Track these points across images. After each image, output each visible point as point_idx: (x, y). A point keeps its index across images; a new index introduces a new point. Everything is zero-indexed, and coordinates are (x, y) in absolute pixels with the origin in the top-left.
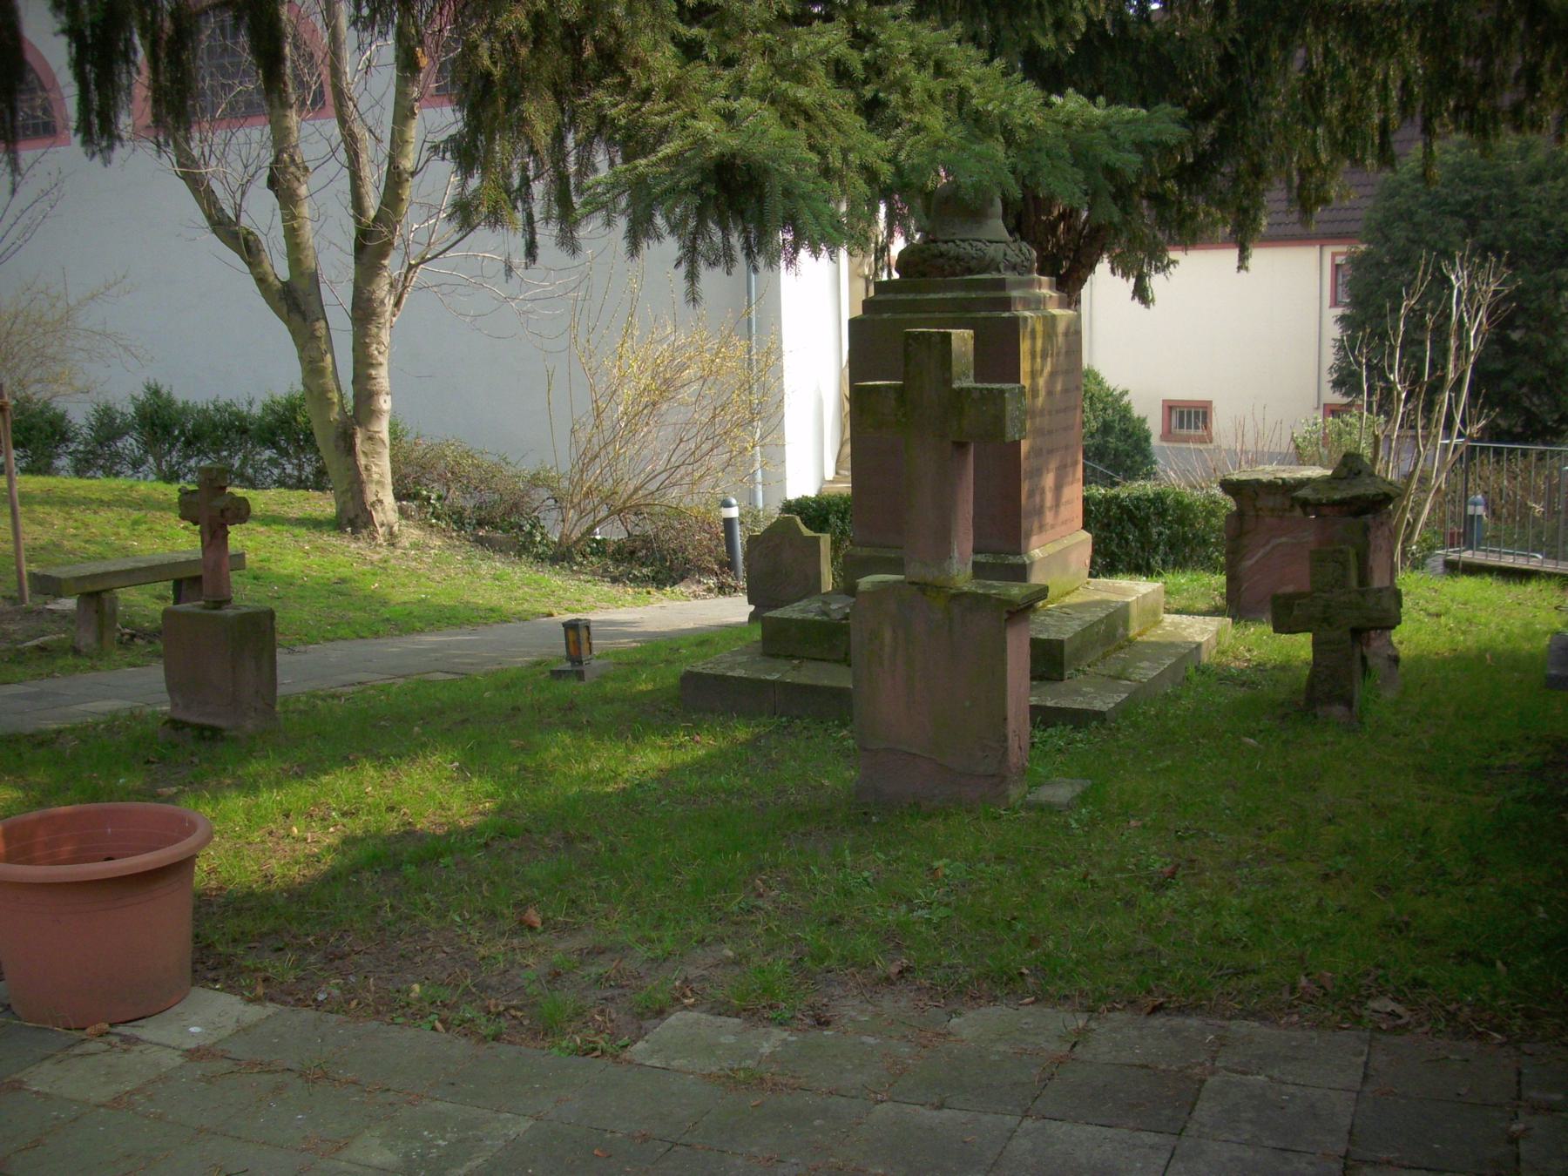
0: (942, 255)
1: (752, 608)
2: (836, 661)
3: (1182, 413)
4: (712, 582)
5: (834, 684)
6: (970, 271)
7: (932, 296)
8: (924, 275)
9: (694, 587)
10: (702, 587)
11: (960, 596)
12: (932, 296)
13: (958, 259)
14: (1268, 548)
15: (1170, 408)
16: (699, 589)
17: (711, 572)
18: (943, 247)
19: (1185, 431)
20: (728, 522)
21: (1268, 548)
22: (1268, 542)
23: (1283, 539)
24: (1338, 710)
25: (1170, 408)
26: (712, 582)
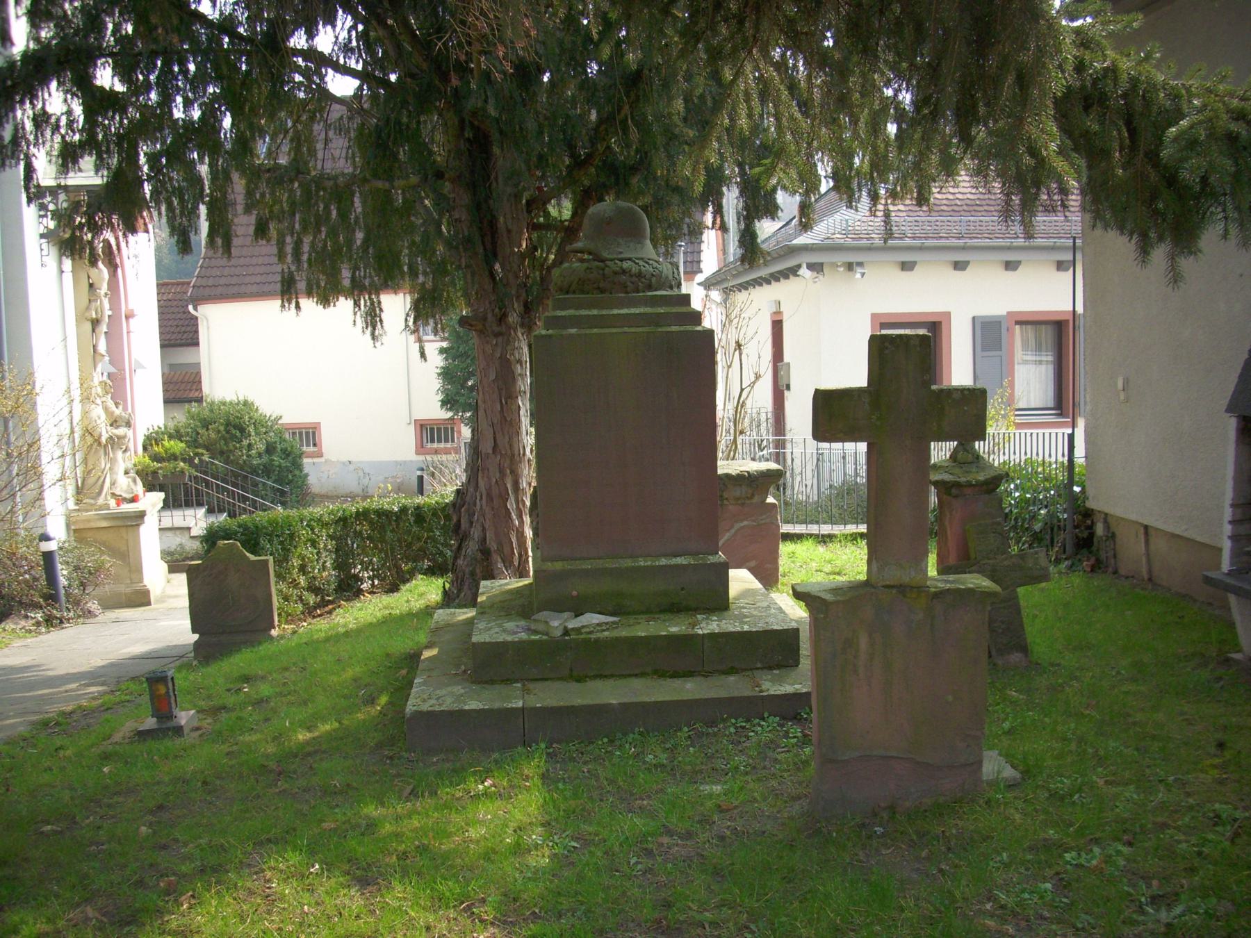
0: (624, 272)
1: (196, 636)
2: (561, 679)
3: (432, 429)
4: (39, 616)
5: (590, 702)
6: (650, 287)
7: (616, 312)
8: (602, 291)
9: (23, 623)
10: (31, 622)
11: (940, 595)
12: (616, 312)
13: (640, 275)
14: (733, 531)
15: (422, 426)
16: (28, 624)
17: (37, 606)
18: (626, 265)
19: (435, 445)
20: (48, 557)
21: (733, 531)
22: (732, 527)
23: (745, 523)
24: (1016, 657)
25: (422, 426)
26: (39, 616)
